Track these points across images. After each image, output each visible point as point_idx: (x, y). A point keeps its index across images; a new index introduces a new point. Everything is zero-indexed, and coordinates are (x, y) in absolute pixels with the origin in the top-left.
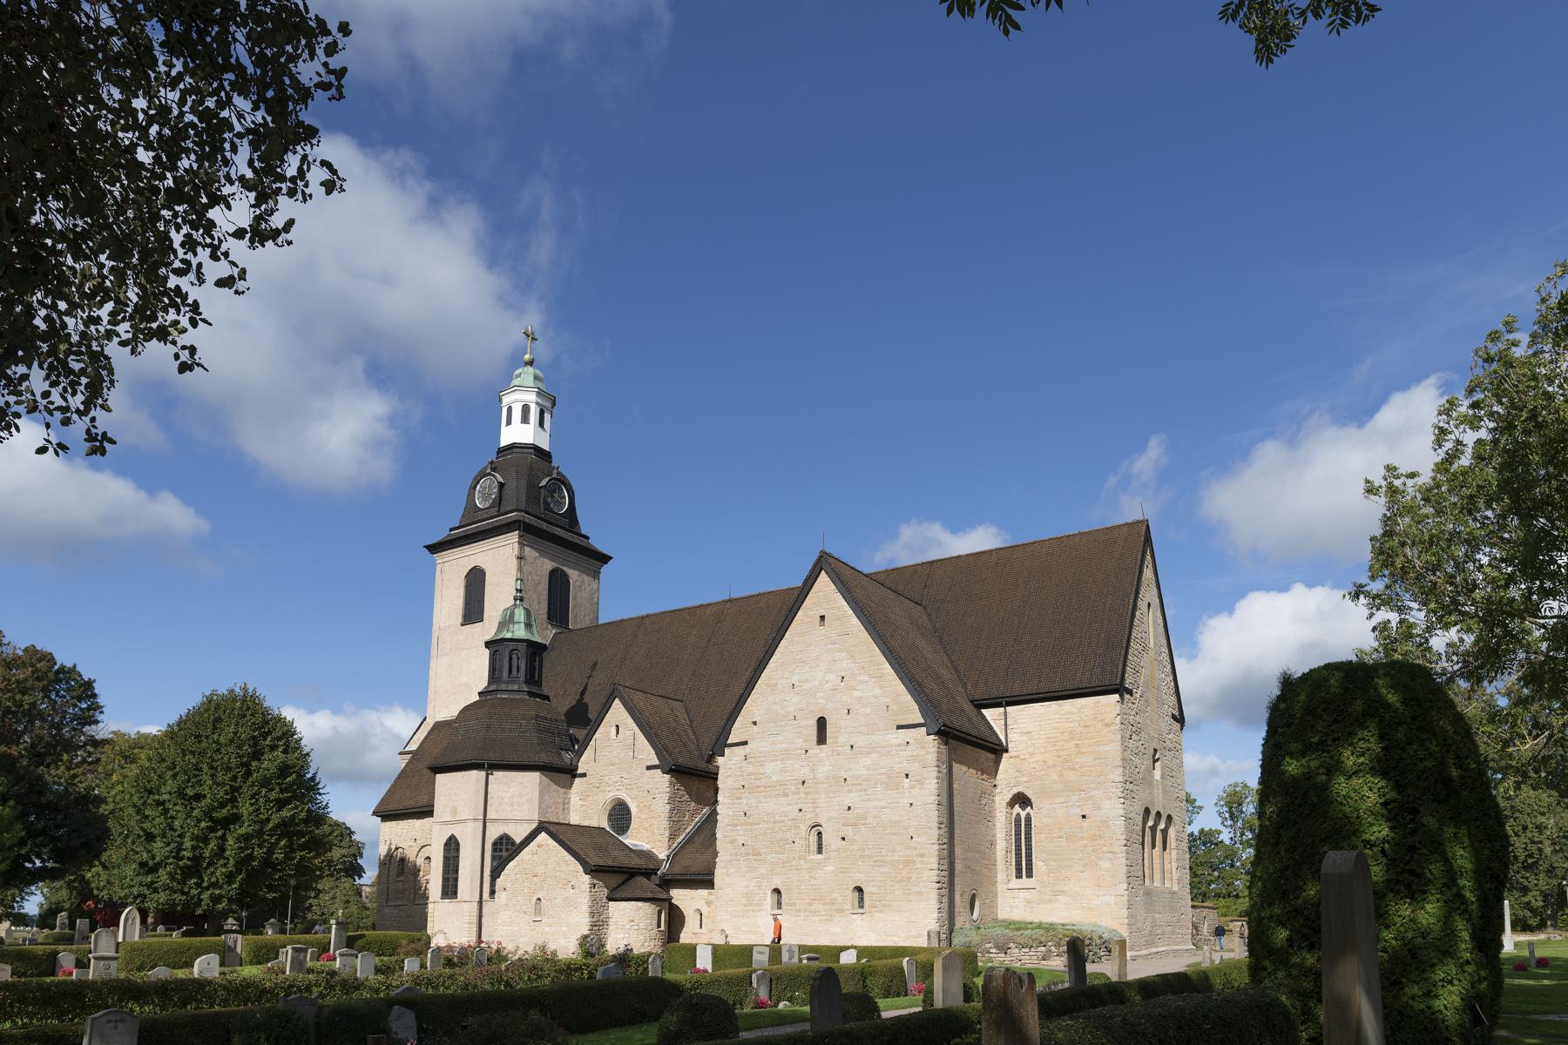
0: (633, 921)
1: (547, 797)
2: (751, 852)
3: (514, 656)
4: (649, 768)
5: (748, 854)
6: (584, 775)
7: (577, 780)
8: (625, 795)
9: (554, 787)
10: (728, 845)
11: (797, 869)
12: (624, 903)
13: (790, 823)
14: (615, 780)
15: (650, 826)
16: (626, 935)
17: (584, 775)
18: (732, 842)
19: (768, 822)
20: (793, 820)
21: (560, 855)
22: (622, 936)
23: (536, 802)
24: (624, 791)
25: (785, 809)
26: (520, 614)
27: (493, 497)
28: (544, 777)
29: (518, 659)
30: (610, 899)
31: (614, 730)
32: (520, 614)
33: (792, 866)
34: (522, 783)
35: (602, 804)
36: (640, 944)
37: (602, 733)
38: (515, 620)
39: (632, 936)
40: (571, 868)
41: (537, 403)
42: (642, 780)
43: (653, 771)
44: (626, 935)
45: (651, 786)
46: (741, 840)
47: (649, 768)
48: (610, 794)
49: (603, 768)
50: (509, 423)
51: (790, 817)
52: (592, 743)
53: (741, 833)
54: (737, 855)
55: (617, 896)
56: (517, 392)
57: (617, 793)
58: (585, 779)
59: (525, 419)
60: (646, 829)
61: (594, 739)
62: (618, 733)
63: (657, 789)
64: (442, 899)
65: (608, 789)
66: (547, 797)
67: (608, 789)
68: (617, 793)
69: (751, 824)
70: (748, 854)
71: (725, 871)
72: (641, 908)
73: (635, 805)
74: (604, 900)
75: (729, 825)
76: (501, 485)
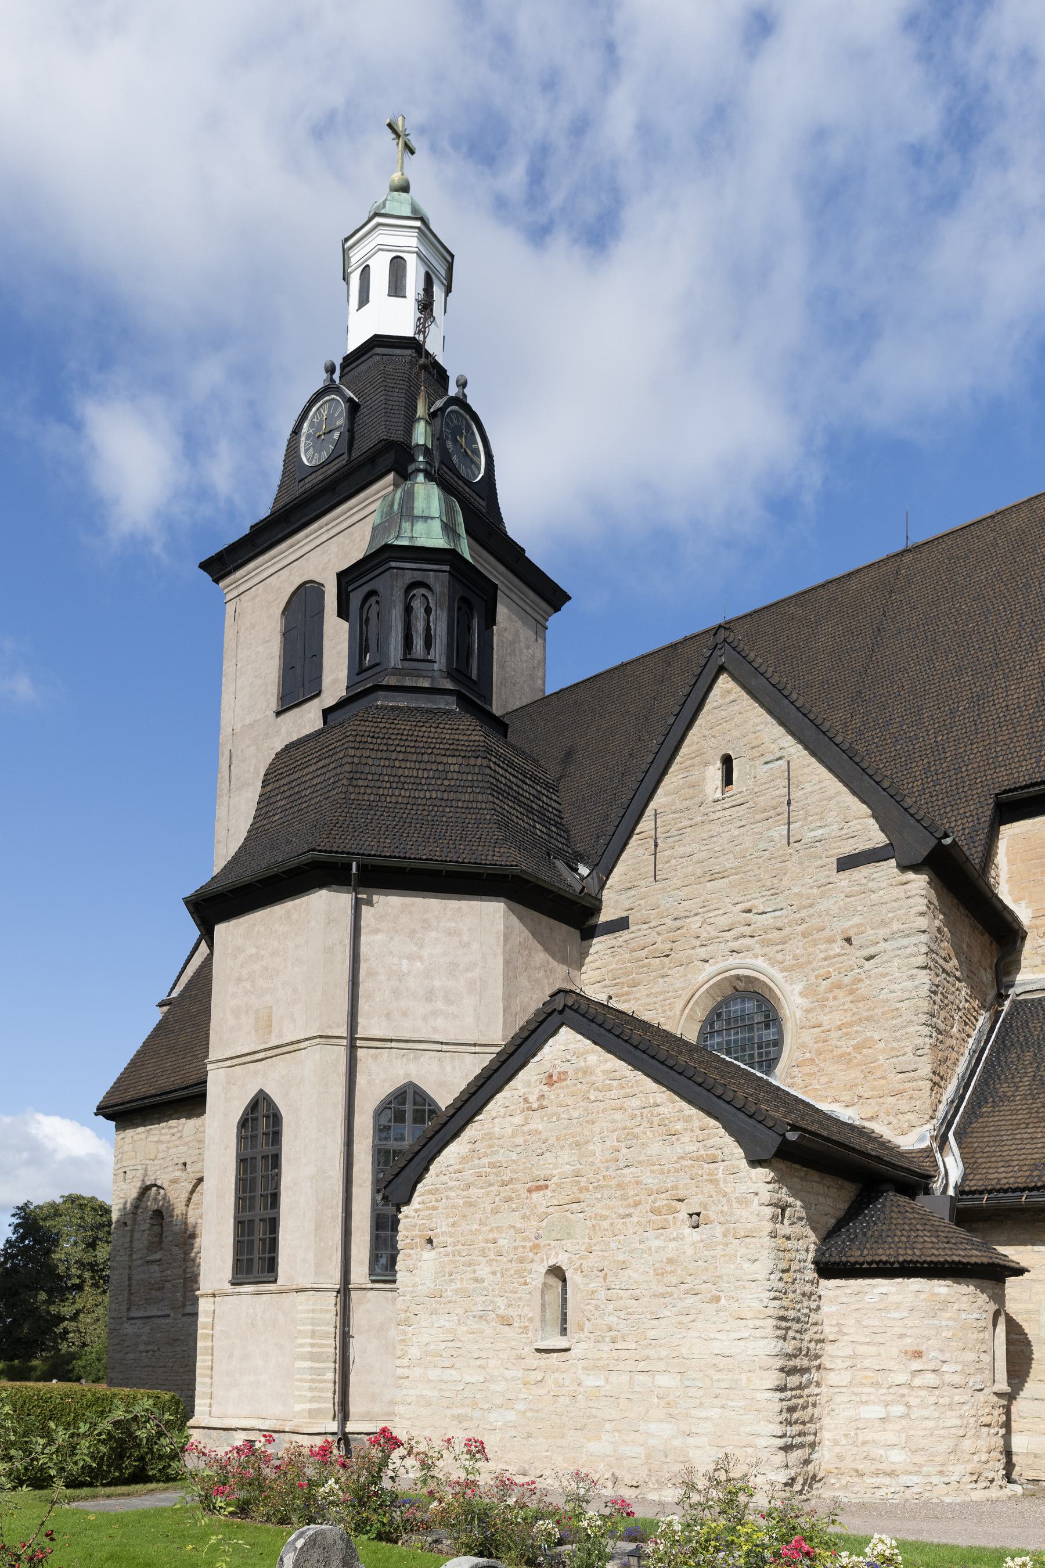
0: (918, 1354)
1: (523, 981)
3: (418, 606)
6: (621, 924)
7: (599, 944)
8: (761, 963)
9: (541, 956)
12: (881, 1285)
14: (723, 921)
15: (858, 1048)
16: (898, 1410)
17: (621, 924)
21: (635, 1102)
22: (879, 1411)
23: (497, 990)
24: (758, 949)
26: (428, 498)
27: (336, 435)
28: (514, 920)
29: (428, 610)
30: (827, 1269)
32: (428, 498)
34: (450, 933)
35: (682, 1003)
36: (944, 1447)
38: (417, 512)
39: (915, 1413)
40: (688, 1145)
41: (419, 255)
42: (824, 905)
44: (898, 1410)
45: (856, 920)
48: (710, 969)
49: (682, 894)
50: (364, 299)
52: (645, 825)
55: (855, 1255)
56: (380, 230)
57: (733, 960)
58: (624, 935)
59: (396, 288)
60: (845, 1060)
61: (649, 811)
62: (728, 780)
63: (883, 923)
65: (702, 953)
66: (523, 981)
67: (702, 953)
68: (733, 960)
72: (947, 1303)
73: (798, 987)
74: (811, 1275)
76: (354, 408)
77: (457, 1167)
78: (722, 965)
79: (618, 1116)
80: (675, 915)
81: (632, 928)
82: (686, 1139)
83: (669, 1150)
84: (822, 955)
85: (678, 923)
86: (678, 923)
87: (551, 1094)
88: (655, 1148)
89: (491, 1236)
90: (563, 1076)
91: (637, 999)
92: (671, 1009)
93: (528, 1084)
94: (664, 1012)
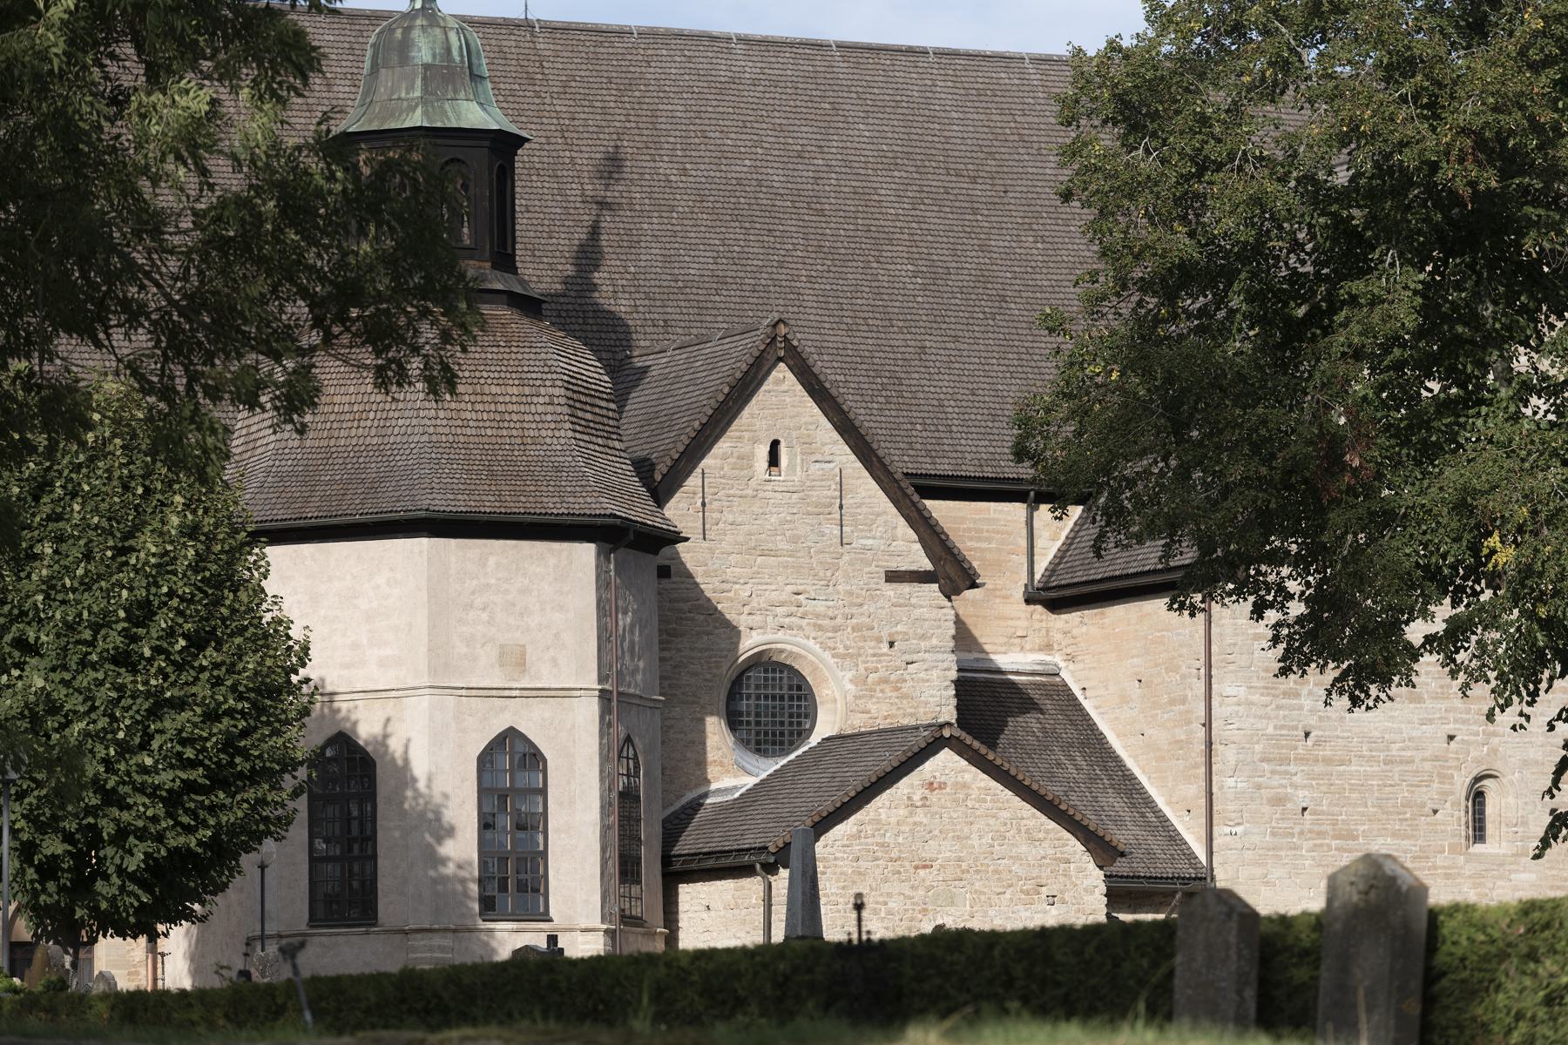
2: (1329, 828)
4: (893, 577)
5: (1321, 834)
10: (1266, 809)
11: (1447, 876)
13: (1427, 766)
18: (1278, 801)
19: (1370, 759)
20: (1436, 758)
25: (1415, 733)
31: (763, 452)
33: (1435, 867)
37: (725, 457)
43: (906, 588)
46: (1302, 797)
47: (893, 577)
51: (1427, 754)
52: (693, 481)
53: (1297, 779)
54: (1292, 835)
64: (312, 927)
69: (1328, 761)
70: (1321, 834)
71: (1258, 871)
75: (1268, 760)
77: (845, 842)
78: (770, 637)
79: (992, 821)
80: (724, 578)
81: (674, 579)
82: (1046, 844)
83: (1034, 851)
84: (871, 651)
85: (725, 586)
86: (725, 586)
87: (934, 797)
88: (1023, 849)
89: (881, 899)
90: (942, 786)
91: (679, 650)
92: (718, 667)
93: (912, 786)
94: (710, 668)
